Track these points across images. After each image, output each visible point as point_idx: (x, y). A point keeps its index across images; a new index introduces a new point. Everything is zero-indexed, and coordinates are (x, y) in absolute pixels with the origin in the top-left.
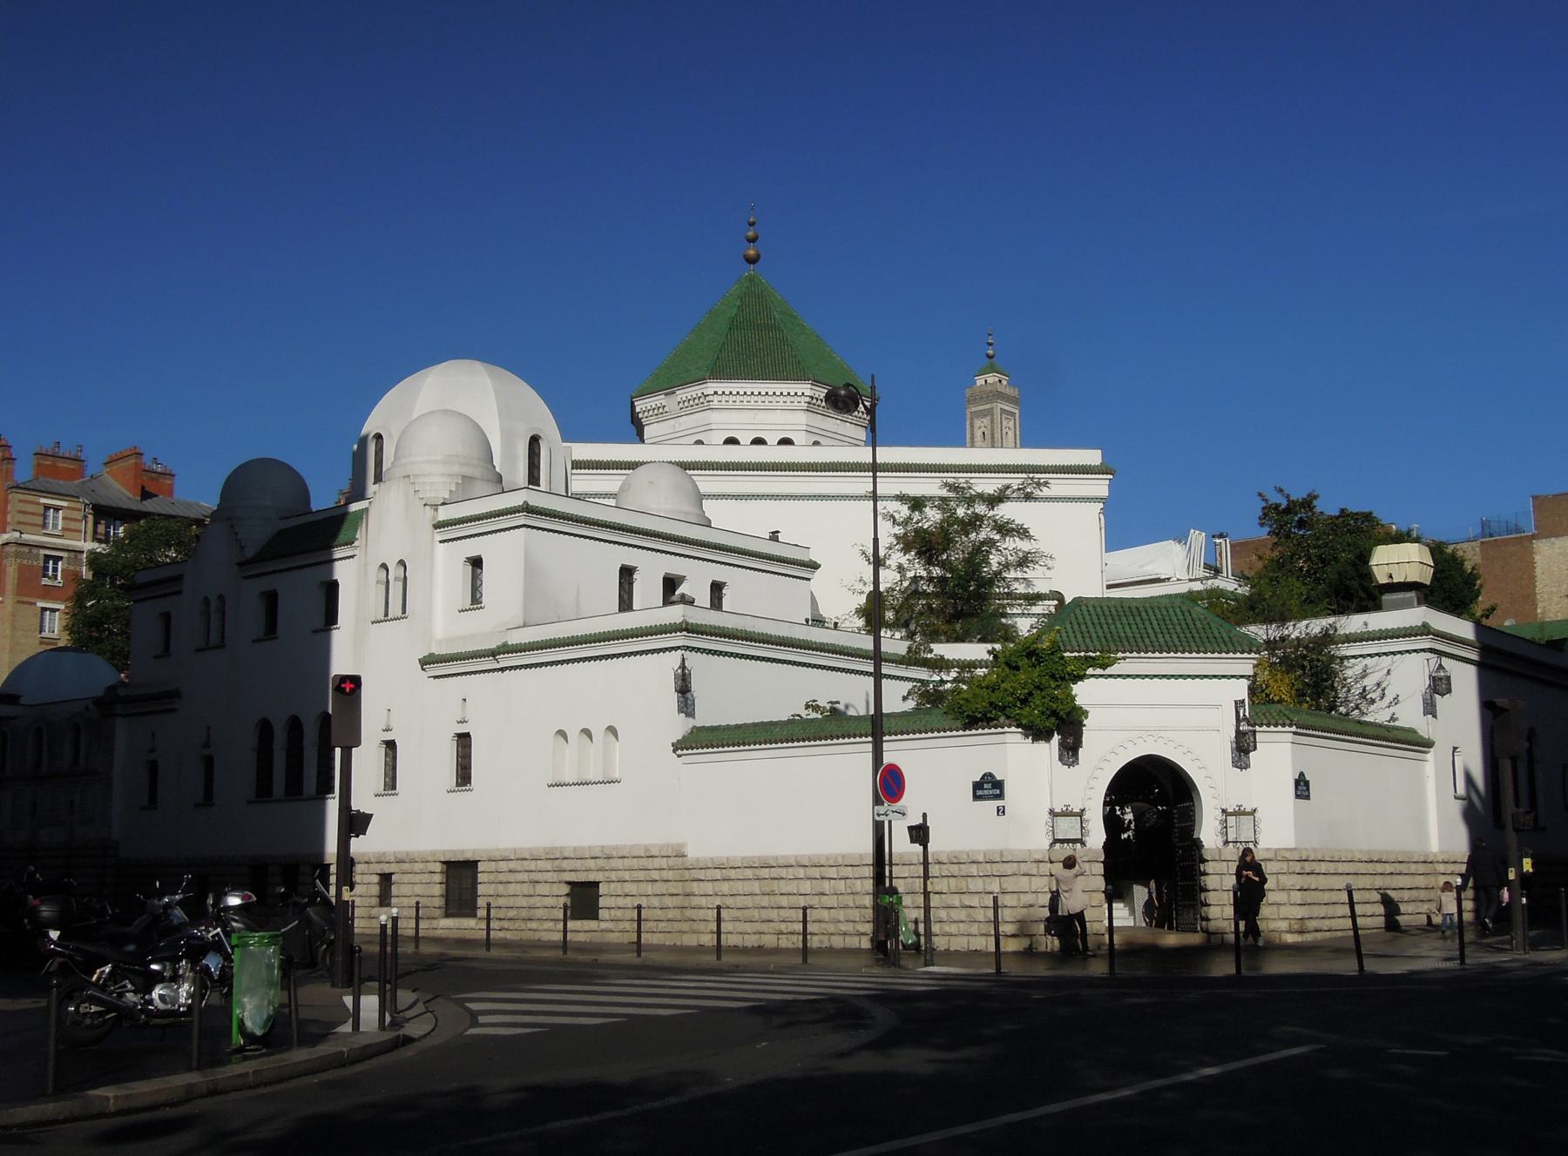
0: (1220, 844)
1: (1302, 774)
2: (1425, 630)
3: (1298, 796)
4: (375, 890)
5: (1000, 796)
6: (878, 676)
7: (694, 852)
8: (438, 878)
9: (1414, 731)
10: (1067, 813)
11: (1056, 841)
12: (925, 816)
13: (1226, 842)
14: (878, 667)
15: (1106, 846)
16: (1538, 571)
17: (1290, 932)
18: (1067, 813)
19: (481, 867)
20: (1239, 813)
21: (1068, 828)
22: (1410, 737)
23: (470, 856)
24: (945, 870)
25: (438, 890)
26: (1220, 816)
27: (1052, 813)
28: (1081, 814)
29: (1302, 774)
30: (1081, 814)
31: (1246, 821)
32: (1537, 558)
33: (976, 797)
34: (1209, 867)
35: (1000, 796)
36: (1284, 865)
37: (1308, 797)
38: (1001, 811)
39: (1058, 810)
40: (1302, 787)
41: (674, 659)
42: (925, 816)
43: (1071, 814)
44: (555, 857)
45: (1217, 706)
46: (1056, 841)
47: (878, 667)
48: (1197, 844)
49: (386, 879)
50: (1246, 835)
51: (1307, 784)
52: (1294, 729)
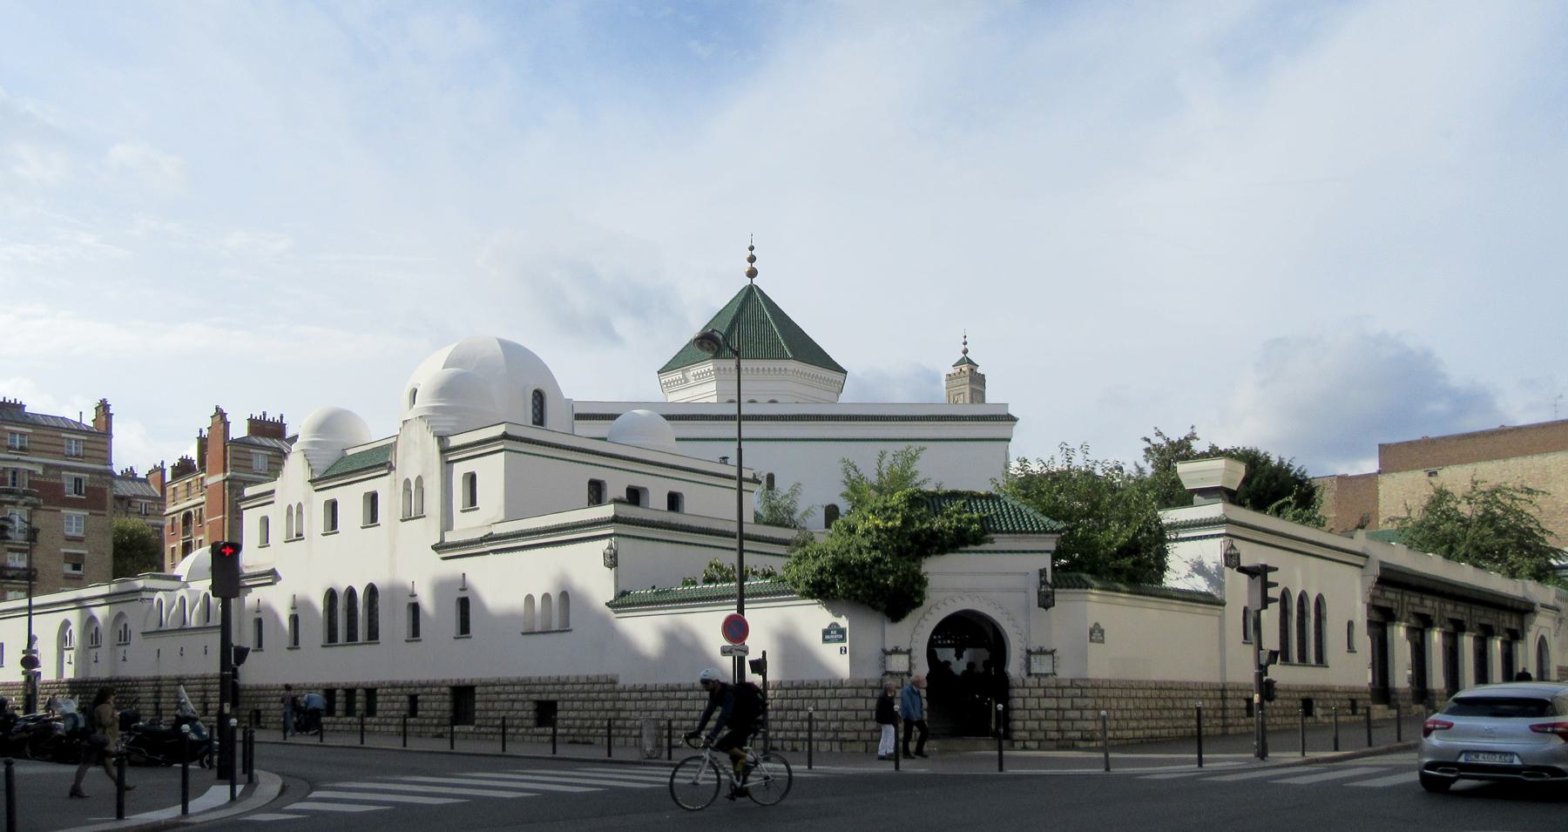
4: (406, 706)
7: (623, 681)
8: (447, 698)
13: (1029, 674)
15: (928, 677)
19: (478, 690)
20: (1042, 652)
23: (467, 682)
25: (447, 706)
26: (1024, 654)
28: (909, 652)
30: (909, 652)
31: (1047, 659)
37: (1102, 641)
39: (889, 649)
44: (526, 683)
46: (887, 673)
49: (413, 699)
50: (1047, 669)
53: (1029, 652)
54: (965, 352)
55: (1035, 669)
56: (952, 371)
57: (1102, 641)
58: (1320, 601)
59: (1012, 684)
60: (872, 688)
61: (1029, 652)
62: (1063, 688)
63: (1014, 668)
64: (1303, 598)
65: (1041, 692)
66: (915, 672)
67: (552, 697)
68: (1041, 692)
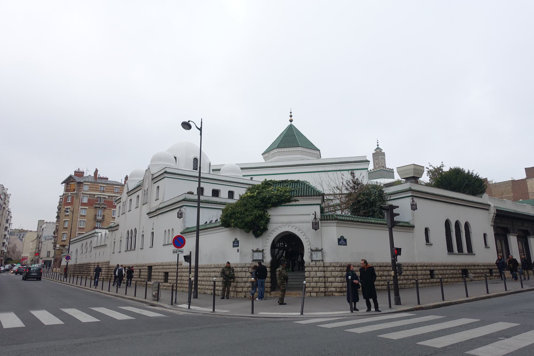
0: (310, 261)
1: (342, 237)
2: (410, 190)
3: (339, 244)
5: (238, 246)
6: (199, 208)
9: (408, 223)
10: (257, 251)
11: (253, 260)
12: (191, 252)
13: (312, 261)
14: (199, 205)
16: (529, 187)
17: (336, 292)
18: (257, 251)
20: (317, 250)
22: (407, 225)
24: (203, 270)
26: (310, 250)
27: (254, 251)
29: (342, 237)
31: (320, 254)
32: (528, 184)
33: (234, 246)
35: (238, 246)
36: (333, 268)
37: (346, 245)
38: (238, 251)
40: (342, 241)
41: (179, 209)
42: (191, 252)
44: (162, 265)
45: (310, 215)
47: (199, 205)
48: (303, 262)
50: (320, 258)
53: (312, 250)
54: (378, 145)
55: (315, 258)
56: (374, 152)
57: (346, 245)
59: (305, 265)
60: (249, 267)
61: (312, 250)
62: (327, 267)
63: (306, 258)
65: (316, 269)
66: (265, 260)
67: (168, 270)
68: (316, 269)
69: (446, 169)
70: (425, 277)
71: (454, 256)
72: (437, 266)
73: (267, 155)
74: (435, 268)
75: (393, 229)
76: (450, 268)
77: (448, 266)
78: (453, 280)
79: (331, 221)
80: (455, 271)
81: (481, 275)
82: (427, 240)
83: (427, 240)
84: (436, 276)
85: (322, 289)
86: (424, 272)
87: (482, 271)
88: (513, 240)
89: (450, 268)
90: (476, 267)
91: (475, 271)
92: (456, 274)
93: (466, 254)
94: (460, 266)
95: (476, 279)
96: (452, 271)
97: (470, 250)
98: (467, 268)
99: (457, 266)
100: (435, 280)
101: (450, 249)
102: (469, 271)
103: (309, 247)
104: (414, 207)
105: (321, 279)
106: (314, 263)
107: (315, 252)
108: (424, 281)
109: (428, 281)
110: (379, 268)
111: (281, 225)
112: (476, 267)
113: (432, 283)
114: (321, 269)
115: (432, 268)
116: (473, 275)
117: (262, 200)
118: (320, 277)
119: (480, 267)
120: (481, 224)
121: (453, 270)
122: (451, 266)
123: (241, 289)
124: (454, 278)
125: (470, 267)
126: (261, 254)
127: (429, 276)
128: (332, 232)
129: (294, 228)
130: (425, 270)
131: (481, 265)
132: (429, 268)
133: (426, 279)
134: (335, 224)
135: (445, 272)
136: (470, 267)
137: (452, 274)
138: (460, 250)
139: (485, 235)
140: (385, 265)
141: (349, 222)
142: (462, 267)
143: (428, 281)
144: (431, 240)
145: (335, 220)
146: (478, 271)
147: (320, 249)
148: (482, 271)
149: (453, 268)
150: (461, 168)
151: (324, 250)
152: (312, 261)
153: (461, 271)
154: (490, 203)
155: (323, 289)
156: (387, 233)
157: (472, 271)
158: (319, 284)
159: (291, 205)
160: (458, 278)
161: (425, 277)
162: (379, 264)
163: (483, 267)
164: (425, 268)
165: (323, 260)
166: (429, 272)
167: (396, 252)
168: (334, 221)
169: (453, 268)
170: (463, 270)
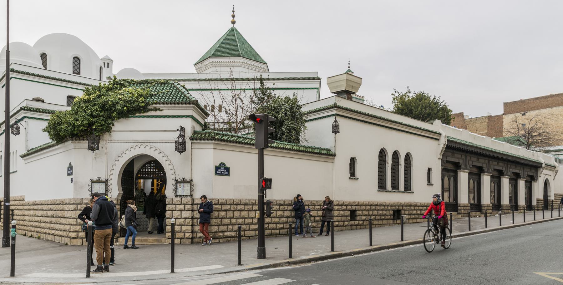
1: (222, 164)
5: (71, 174)
9: (329, 150)
10: (99, 181)
13: (176, 196)
18: (99, 181)
20: (184, 181)
21: (99, 189)
26: (174, 182)
30: (107, 181)
31: (187, 186)
34: (168, 207)
35: (71, 174)
37: (228, 175)
39: (95, 180)
40: (222, 170)
43: (102, 182)
48: (164, 197)
50: (187, 192)
51: (227, 169)
52: (213, 142)
53: (177, 182)
55: (180, 192)
57: (228, 175)
58: (408, 157)
59: (167, 201)
61: (177, 182)
63: (169, 192)
64: (396, 155)
65: (182, 207)
68: (182, 207)
69: (412, 95)
70: (343, 218)
71: (385, 193)
72: (361, 206)
73: (199, 66)
74: (358, 208)
75: (265, 152)
76: (379, 208)
77: (375, 206)
78: (380, 222)
79: (206, 141)
80: (385, 212)
81: (417, 216)
82: (352, 173)
83: (352, 173)
84: (358, 218)
85: (187, 235)
86: (342, 213)
87: (419, 212)
88: (463, 177)
89: (379, 208)
90: (412, 208)
91: (411, 212)
92: (385, 215)
93: (402, 192)
94: (391, 206)
95: (411, 221)
96: (380, 212)
97: (408, 188)
98: (401, 208)
99: (388, 206)
100: (356, 222)
101: (382, 186)
102: (403, 212)
103: (174, 177)
104: (336, 129)
105: (187, 221)
106: (179, 199)
107: (182, 185)
108: (341, 223)
109: (347, 223)
110: (278, 207)
111: (135, 144)
112: (412, 208)
113: (352, 225)
114: (187, 207)
115: (354, 208)
116: (407, 217)
117: (104, 107)
118: (186, 218)
119: (417, 208)
120: (426, 156)
121: (382, 210)
122: (381, 205)
123: (76, 234)
124: (383, 220)
125: (404, 208)
126: (103, 186)
127: (349, 218)
128: (207, 156)
129: (153, 149)
130: (344, 210)
131: (419, 204)
132: (350, 207)
133: (344, 221)
134: (212, 146)
135: (371, 213)
136: (404, 208)
137: (380, 215)
138: (395, 187)
139: (429, 170)
140: (286, 203)
141: (235, 144)
142: (394, 208)
143: (347, 223)
144: (358, 173)
145: (211, 140)
146: (414, 212)
147: (188, 180)
148: (419, 212)
149: (382, 208)
150: (426, 92)
151: (194, 182)
152: (176, 196)
153: (392, 212)
154: (441, 131)
155: (189, 234)
156: (255, 157)
157: (407, 212)
158: (184, 228)
159: (149, 116)
160: (388, 219)
161: (343, 218)
162: (278, 202)
163: (421, 208)
164: (344, 207)
165: (191, 196)
166: (348, 213)
167: (265, 184)
168: (210, 142)
169: (382, 208)
170: (394, 211)
